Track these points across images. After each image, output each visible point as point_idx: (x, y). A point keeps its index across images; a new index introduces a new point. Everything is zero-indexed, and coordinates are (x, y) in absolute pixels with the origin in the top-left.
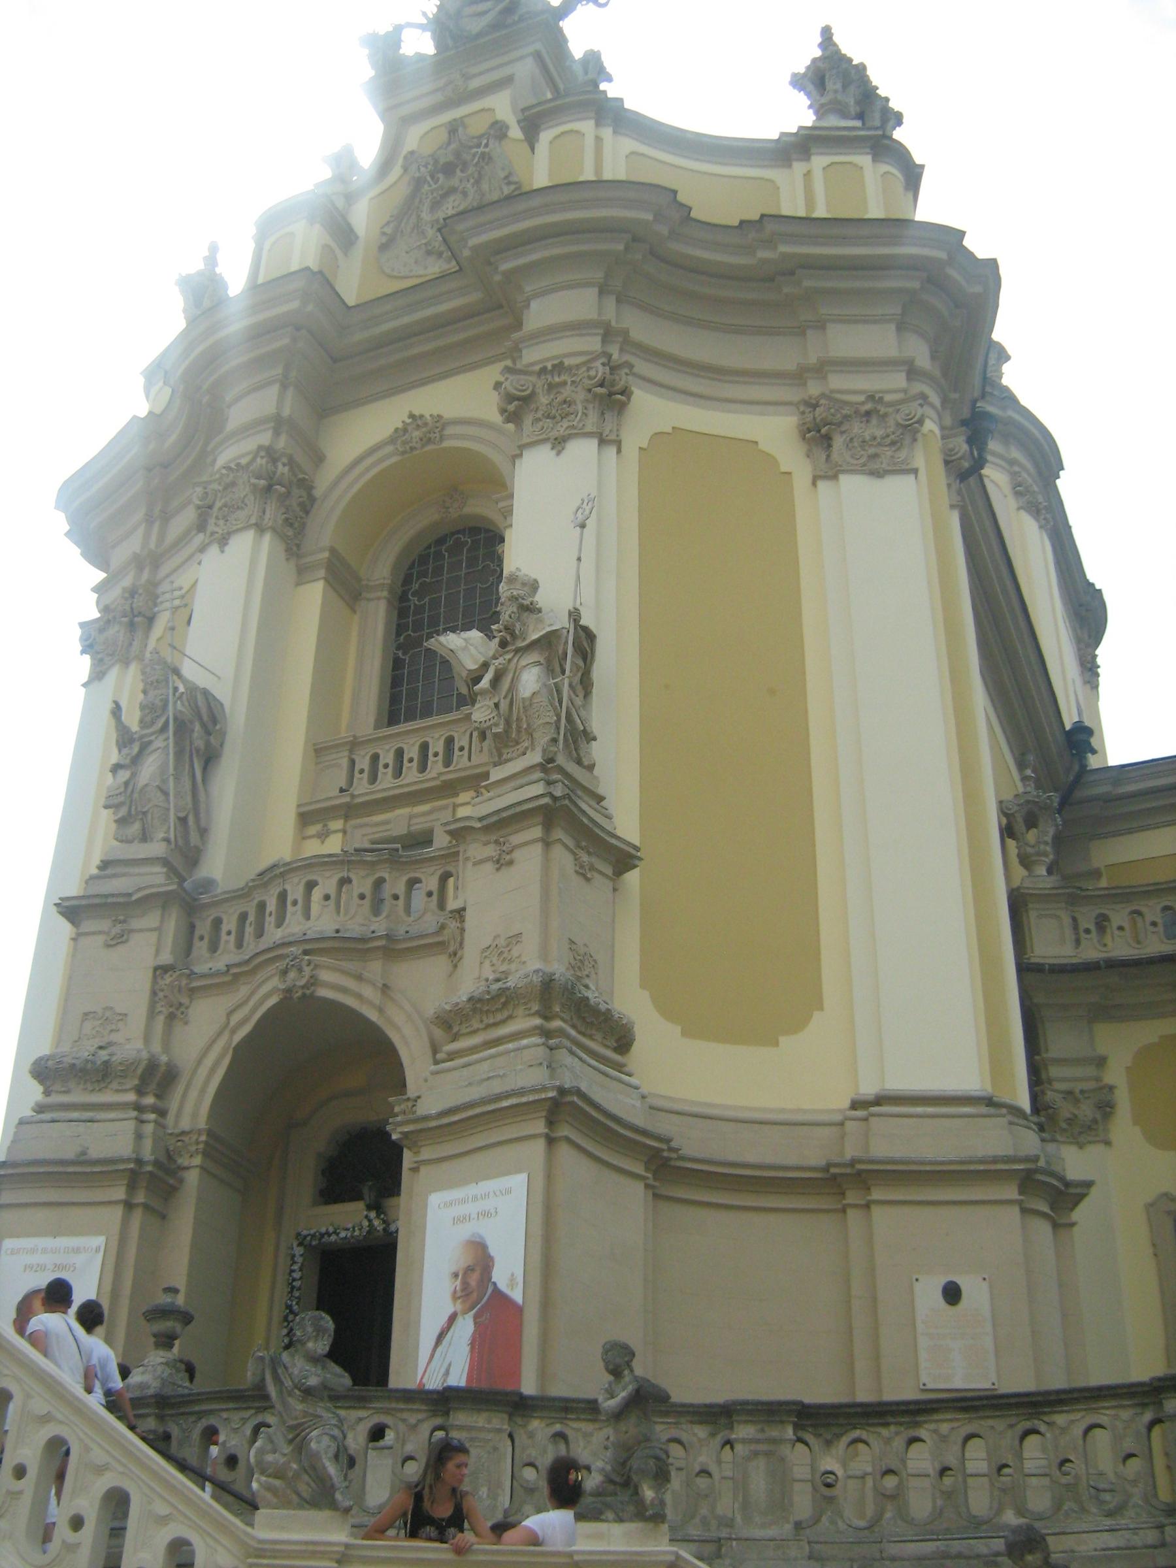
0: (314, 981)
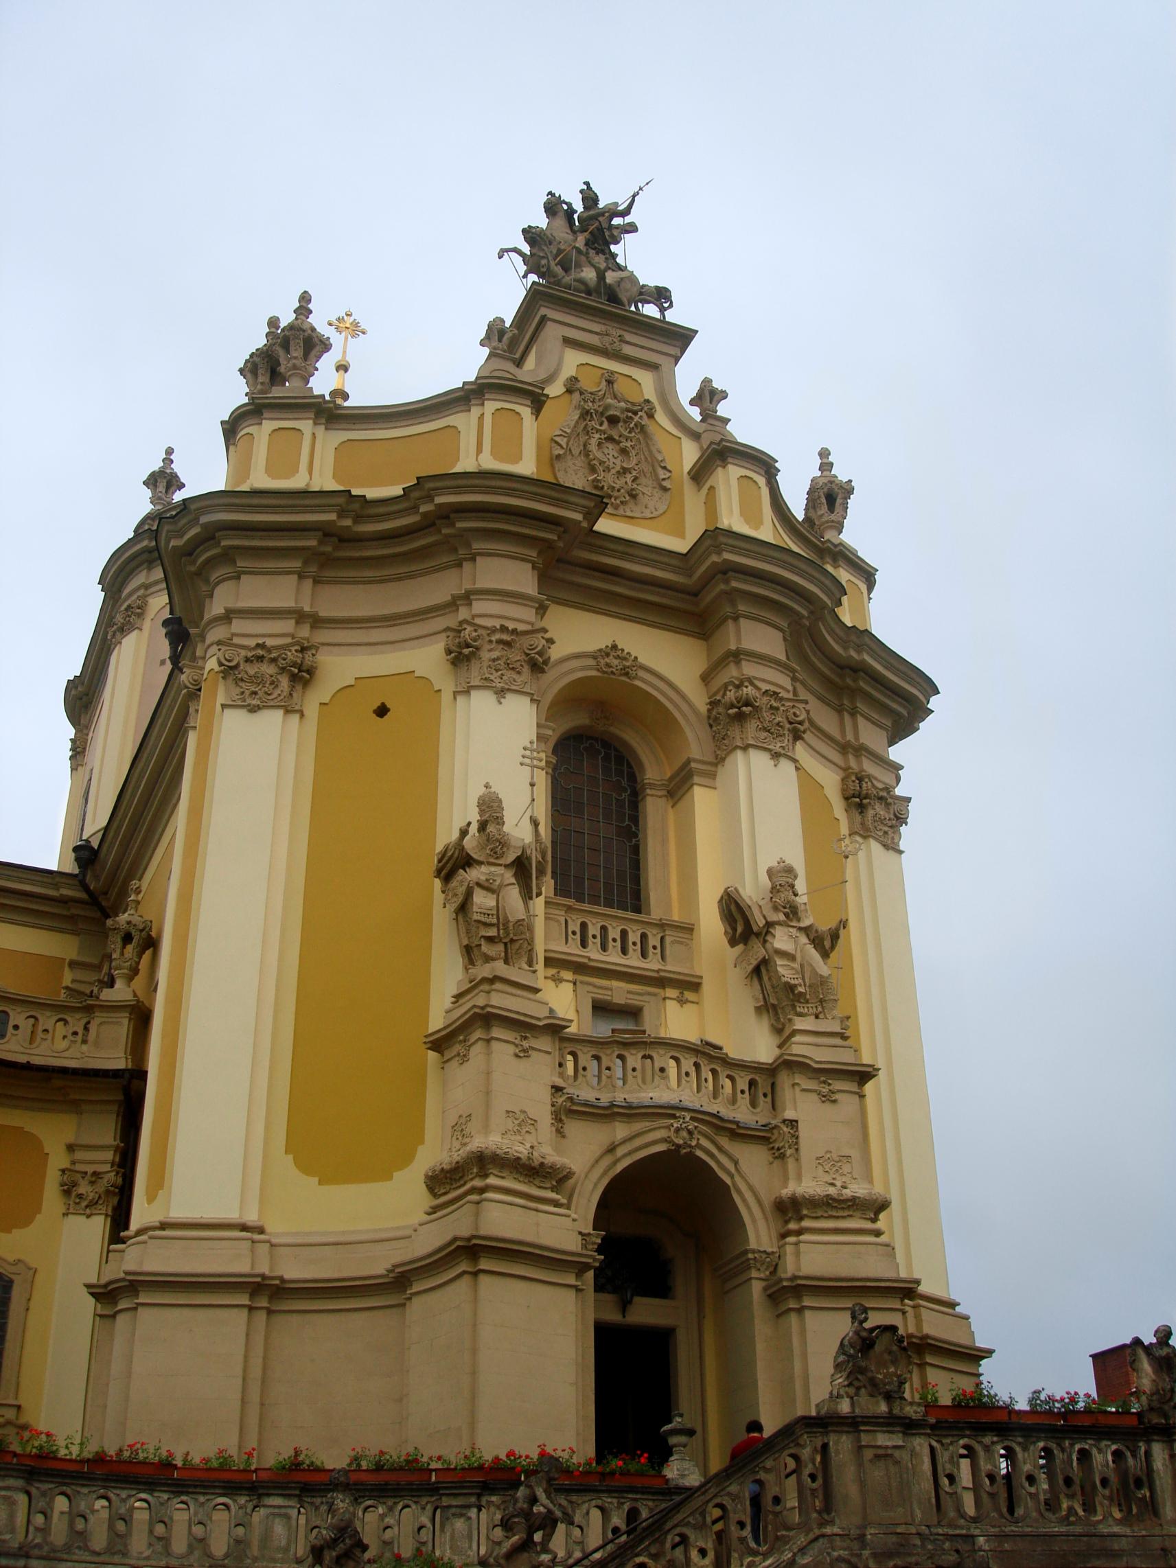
0: (699, 1146)
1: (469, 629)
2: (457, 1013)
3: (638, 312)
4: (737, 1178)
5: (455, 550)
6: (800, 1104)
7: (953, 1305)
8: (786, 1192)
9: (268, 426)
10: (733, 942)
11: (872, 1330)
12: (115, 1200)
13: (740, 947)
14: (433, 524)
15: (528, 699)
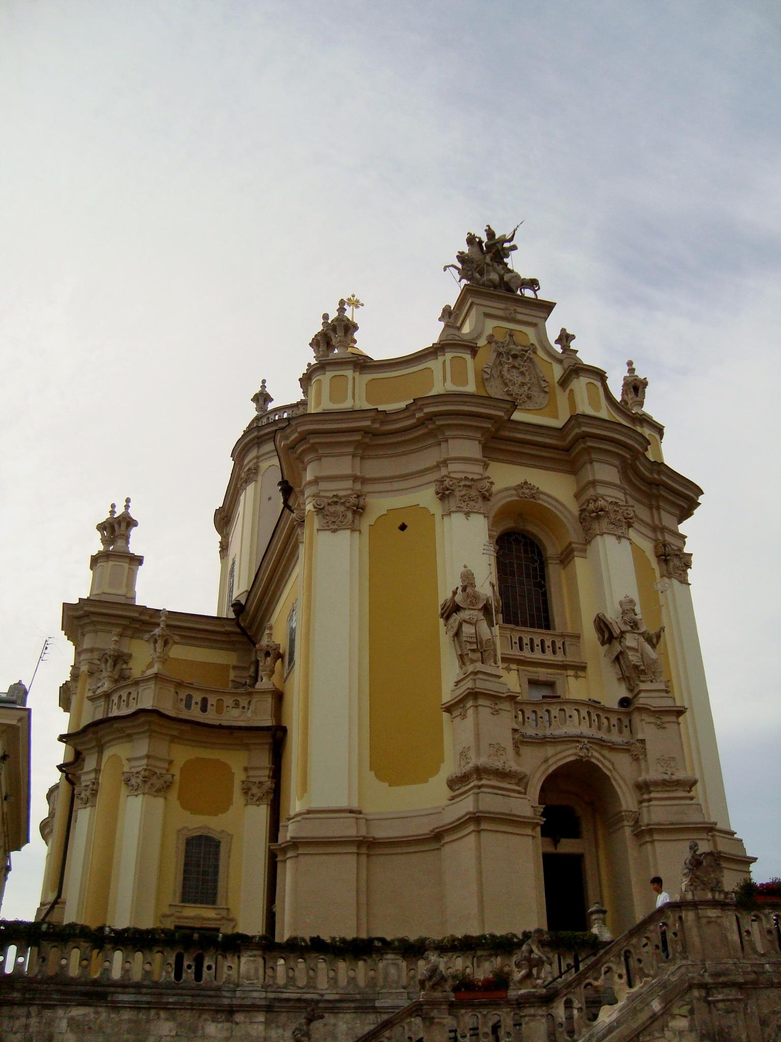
0: (593, 756)
1: (448, 480)
2: (458, 692)
3: (523, 295)
4: (615, 774)
5: (436, 436)
6: (645, 729)
7: (733, 834)
8: (640, 779)
9: (329, 374)
10: (603, 643)
11: (701, 855)
12: (271, 796)
13: (607, 646)
14: (423, 424)
15: (482, 516)
